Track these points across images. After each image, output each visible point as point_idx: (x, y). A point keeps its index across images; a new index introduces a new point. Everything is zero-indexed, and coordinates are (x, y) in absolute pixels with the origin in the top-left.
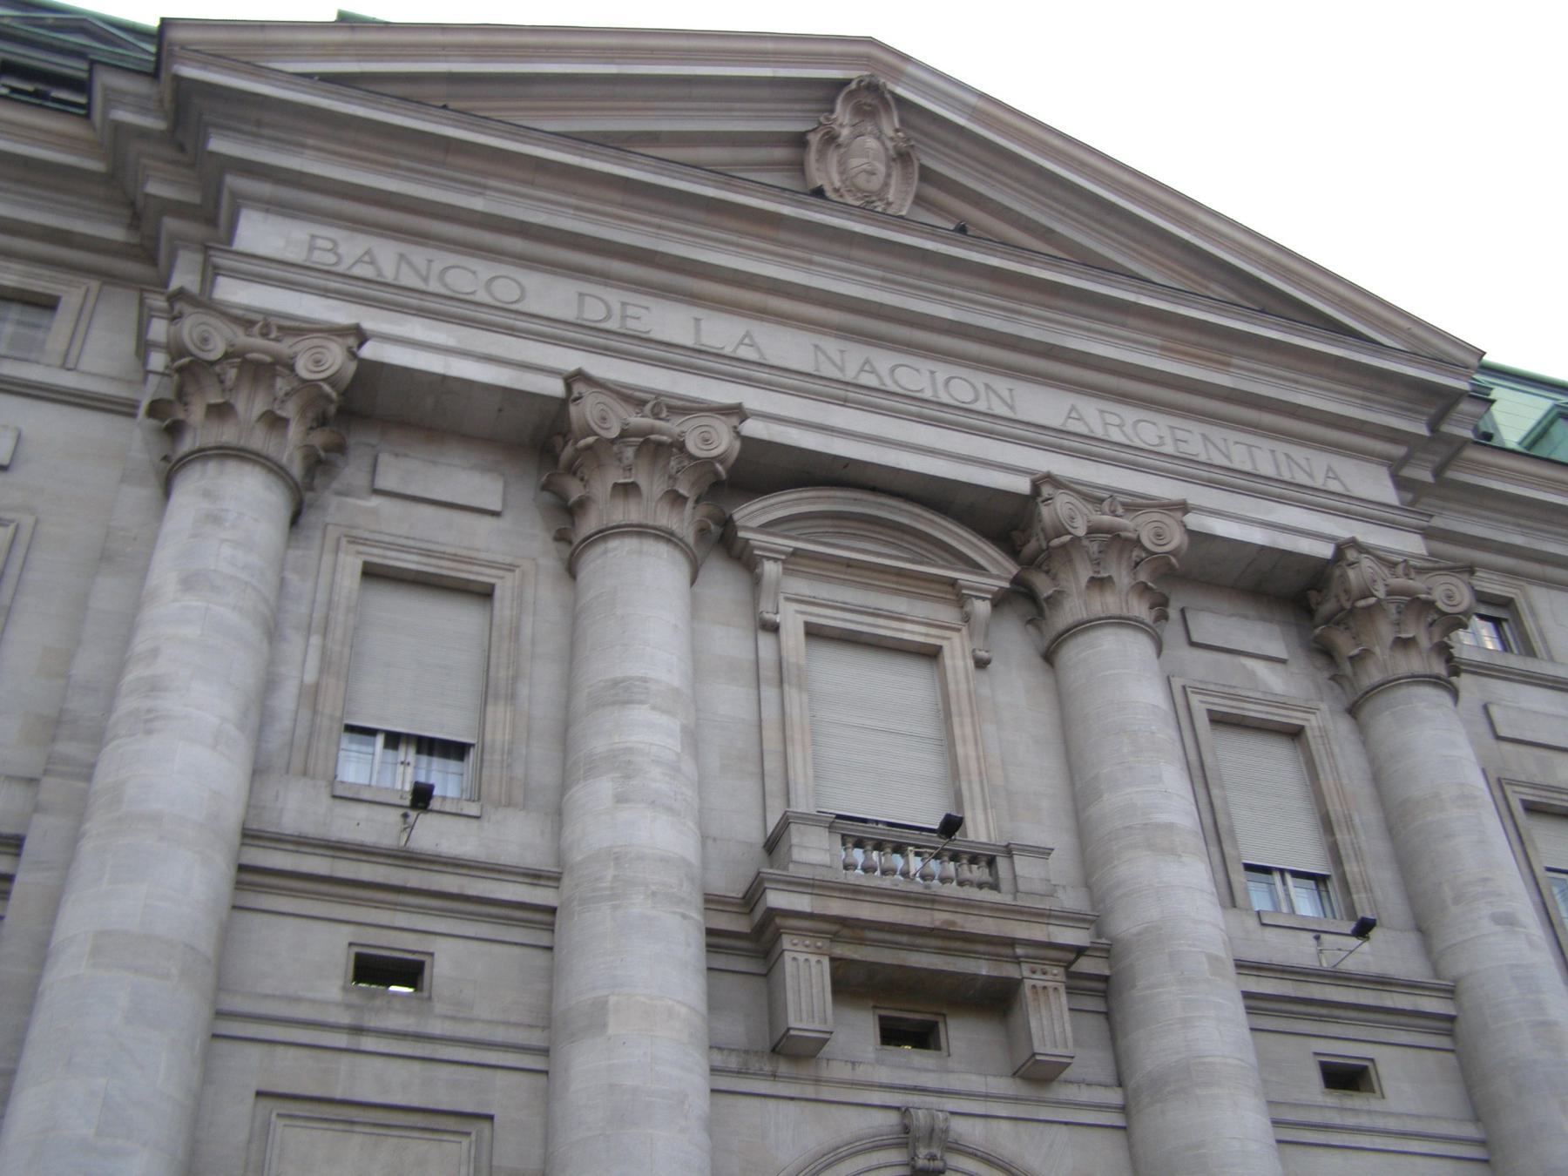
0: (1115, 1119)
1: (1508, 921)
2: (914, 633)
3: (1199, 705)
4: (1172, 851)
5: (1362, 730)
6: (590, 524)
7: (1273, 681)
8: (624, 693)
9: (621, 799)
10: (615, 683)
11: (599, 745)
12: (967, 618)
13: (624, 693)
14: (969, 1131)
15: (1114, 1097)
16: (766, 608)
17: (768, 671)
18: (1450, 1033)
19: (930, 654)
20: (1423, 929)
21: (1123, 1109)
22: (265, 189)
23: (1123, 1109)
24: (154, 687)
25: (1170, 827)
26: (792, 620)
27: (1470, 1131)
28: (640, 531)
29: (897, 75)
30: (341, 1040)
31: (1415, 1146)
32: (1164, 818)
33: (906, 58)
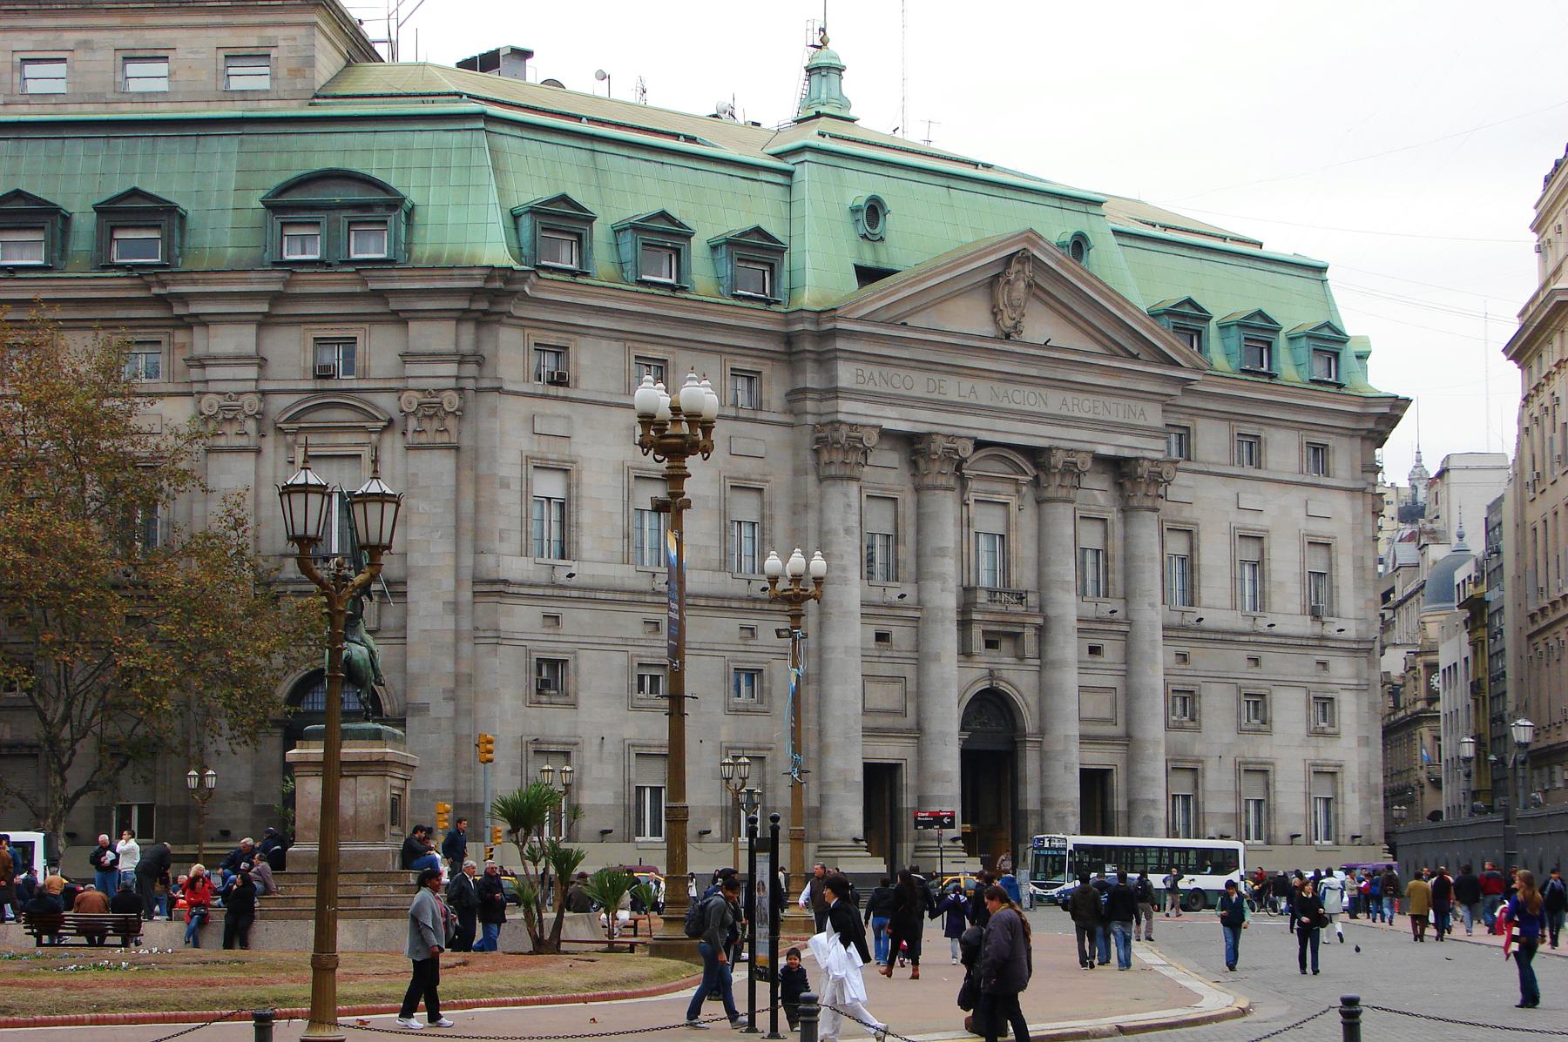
0: (1038, 669)
1: (1152, 605)
2: (1002, 499)
3: (1078, 515)
4: (1068, 591)
5: (1126, 523)
6: (928, 481)
7: (1101, 498)
8: (941, 552)
9: (942, 590)
10: (940, 548)
11: (935, 570)
12: (1018, 491)
13: (941, 552)
14: (1005, 674)
15: (1037, 662)
16: (965, 497)
17: (965, 522)
18: (1126, 635)
19: (1006, 504)
20: (1126, 598)
21: (1040, 666)
22: (846, 355)
23: (1040, 666)
24: (844, 569)
25: (1069, 581)
26: (971, 502)
27: (1124, 667)
28: (947, 489)
29: (1035, 244)
30: (876, 660)
31: (1108, 672)
32: (1068, 579)
33: (1041, 237)
